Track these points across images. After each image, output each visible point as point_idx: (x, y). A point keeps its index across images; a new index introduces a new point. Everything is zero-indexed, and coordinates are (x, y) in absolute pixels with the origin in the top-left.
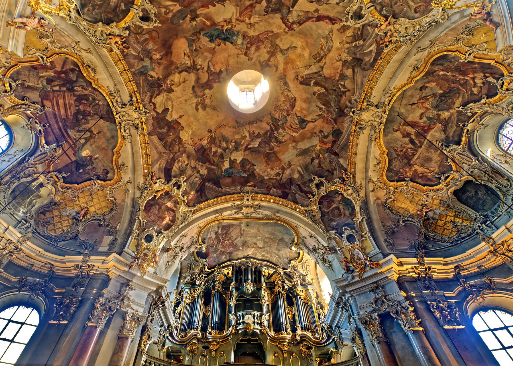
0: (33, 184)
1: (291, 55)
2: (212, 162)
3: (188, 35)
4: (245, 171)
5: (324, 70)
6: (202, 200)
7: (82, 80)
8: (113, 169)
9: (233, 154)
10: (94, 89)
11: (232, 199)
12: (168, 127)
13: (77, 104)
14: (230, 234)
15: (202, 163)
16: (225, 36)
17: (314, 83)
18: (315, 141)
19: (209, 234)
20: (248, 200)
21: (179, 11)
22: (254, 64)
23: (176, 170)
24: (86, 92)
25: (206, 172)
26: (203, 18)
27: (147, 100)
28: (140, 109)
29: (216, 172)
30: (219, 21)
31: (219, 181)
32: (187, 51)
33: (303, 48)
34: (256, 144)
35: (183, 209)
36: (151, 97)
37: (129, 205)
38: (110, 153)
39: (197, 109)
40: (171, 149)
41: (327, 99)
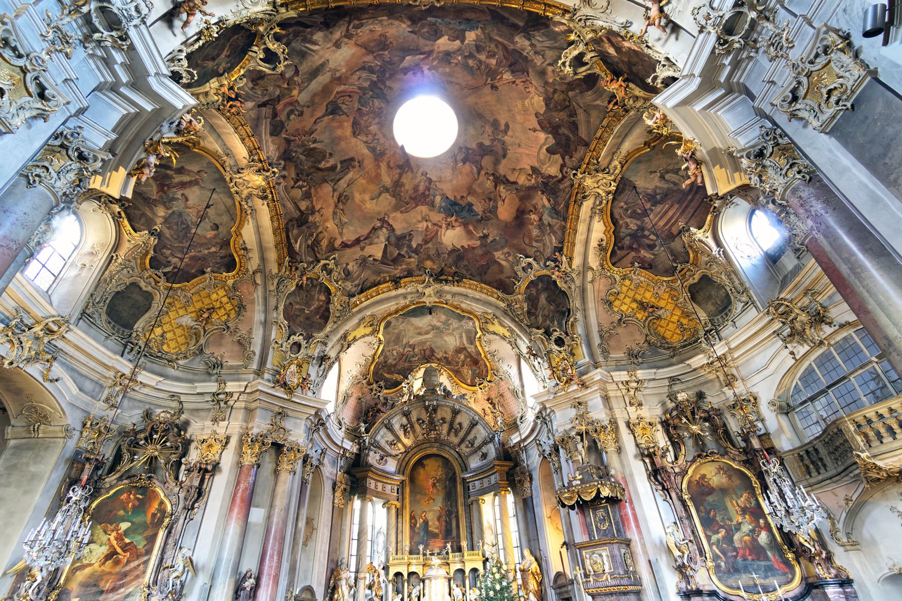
5: (331, 189)
9: (456, 47)
15: (521, 54)
24: (628, 220)
27: (567, 183)
32: (500, 203)
36: (560, 181)
39: (507, 126)
40: (567, 103)
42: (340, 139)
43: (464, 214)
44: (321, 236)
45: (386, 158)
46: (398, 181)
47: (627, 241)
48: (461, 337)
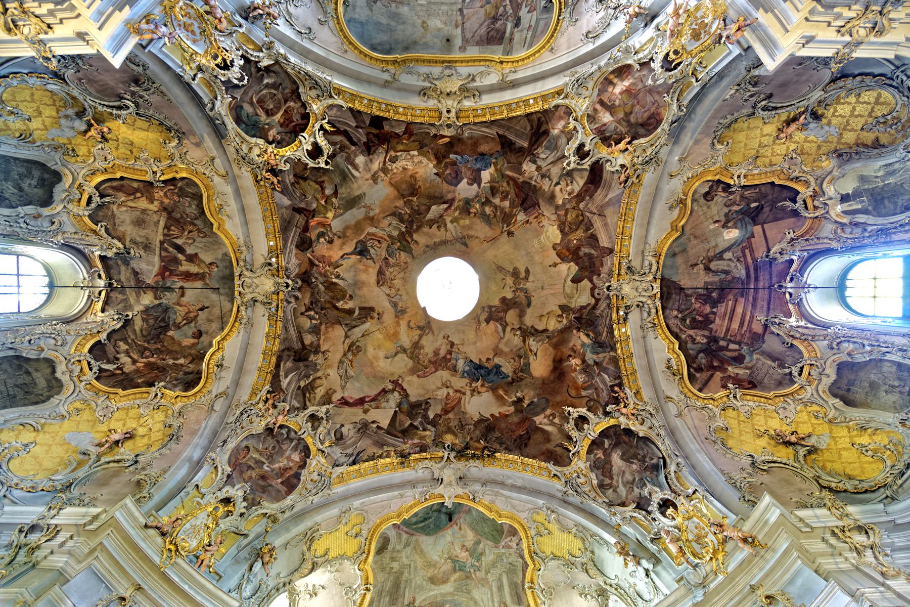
0: (860, 206)
1: (391, 347)
2: (511, 182)
3: (529, 380)
4: (454, 163)
6: (540, 115)
7: (691, 352)
8: (694, 200)
9: (474, 193)
10: (677, 337)
11: (479, 112)
12: (578, 254)
13: (712, 316)
14: (487, 15)
15: (530, 184)
16: (481, 373)
17: (354, 312)
18: (337, 225)
19: (533, 23)
20: (448, 111)
21: (537, 414)
22: (440, 329)
23: (578, 179)
24: (691, 332)
25: (524, 167)
26: (507, 401)
27: (603, 305)
28: (617, 296)
29: (506, 165)
30: (487, 394)
31: (503, 148)
32: (532, 358)
33: (376, 358)
34: (435, 210)
35: (581, 105)
36: (595, 307)
37: (689, 134)
38: (687, 229)
39: (527, 271)
41: (331, 294)
42: (363, 283)
43: (492, 377)
44: (318, 382)
45: (407, 317)
46: (418, 342)
47: (702, 359)
48: (500, 588)
